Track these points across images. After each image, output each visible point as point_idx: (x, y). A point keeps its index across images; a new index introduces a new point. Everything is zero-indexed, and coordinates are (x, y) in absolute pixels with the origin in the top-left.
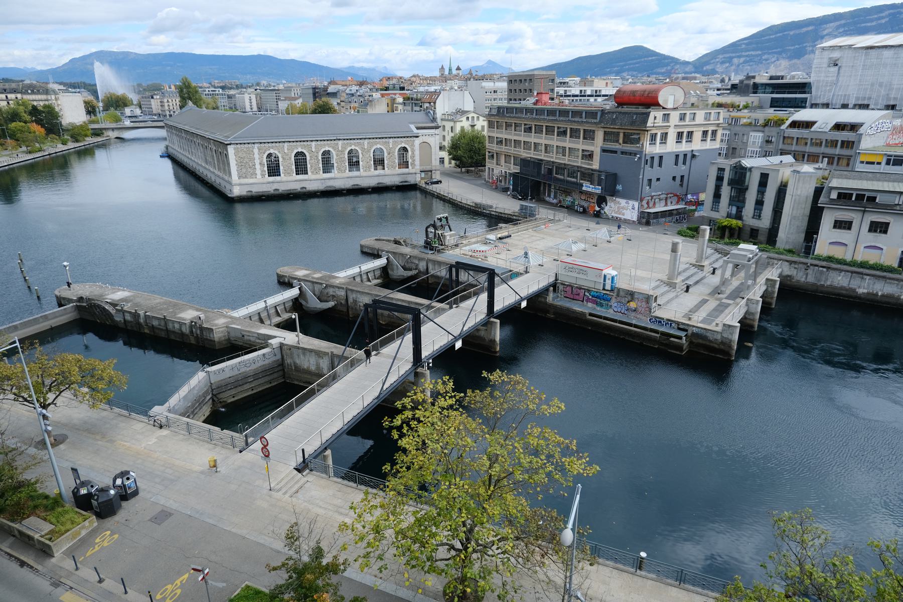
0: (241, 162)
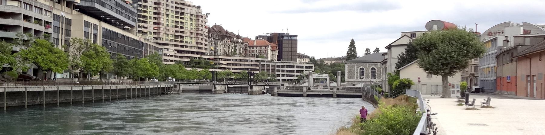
0: (350, 71)
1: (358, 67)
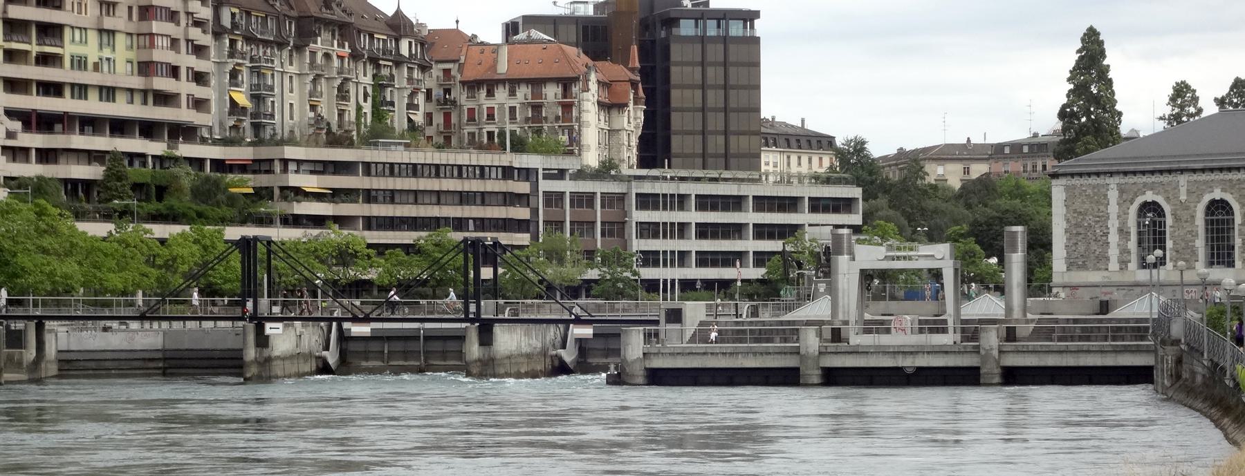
0: (1077, 225)
1: (1126, 197)
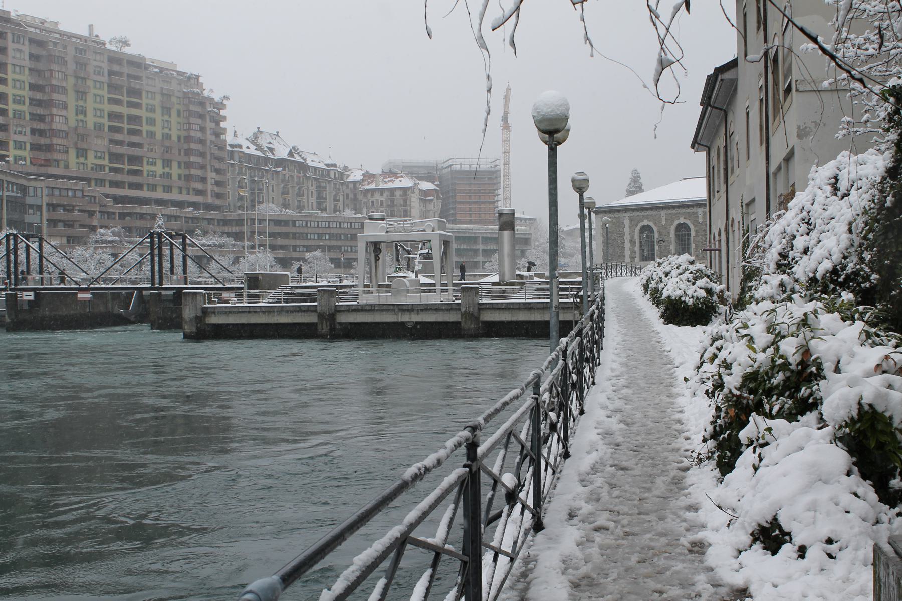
1: (633, 226)
